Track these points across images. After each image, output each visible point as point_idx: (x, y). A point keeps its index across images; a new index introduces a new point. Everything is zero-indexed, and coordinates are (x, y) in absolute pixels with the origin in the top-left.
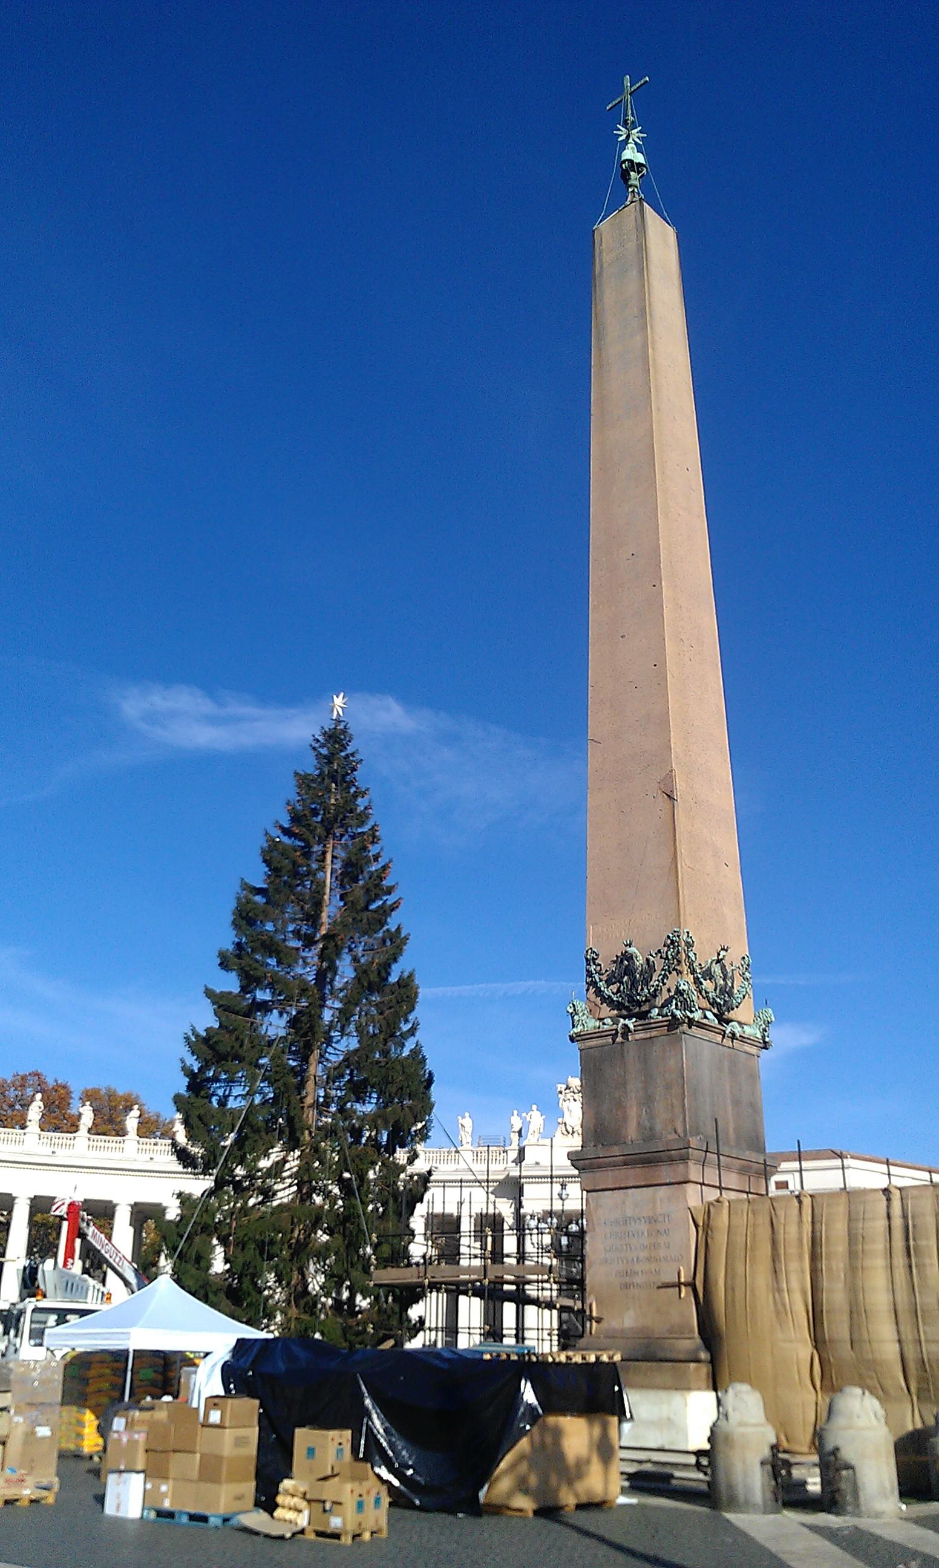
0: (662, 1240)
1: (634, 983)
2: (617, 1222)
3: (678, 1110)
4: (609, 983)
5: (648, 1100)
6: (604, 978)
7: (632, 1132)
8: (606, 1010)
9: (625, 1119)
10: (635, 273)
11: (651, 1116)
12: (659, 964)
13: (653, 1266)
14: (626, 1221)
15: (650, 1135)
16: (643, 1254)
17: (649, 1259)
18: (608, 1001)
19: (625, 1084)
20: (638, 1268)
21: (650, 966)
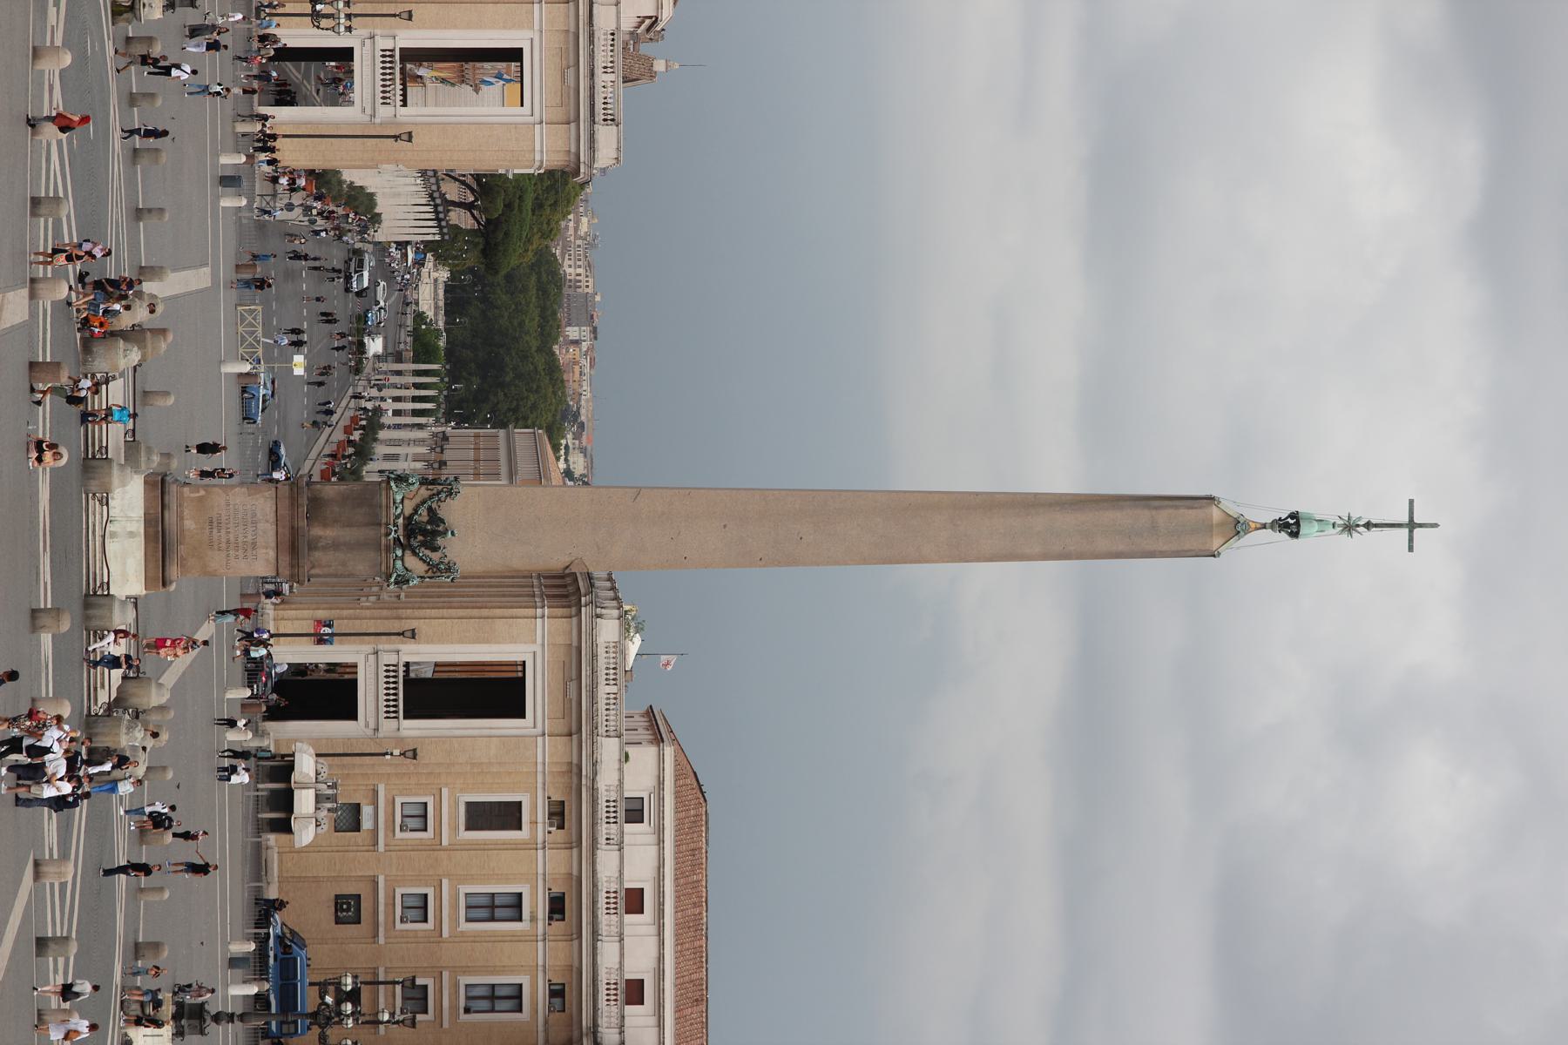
0: (240, 552)
1: (424, 532)
2: (254, 515)
3: (326, 570)
4: (430, 509)
5: (336, 546)
6: (434, 506)
7: (317, 531)
8: (408, 512)
9: (325, 526)
10: (1121, 548)
11: (325, 548)
12: (435, 556)
13: (223, 545)
14: (255, 523)
15: (312, 546)
16: (232, 537)
17: (228, 542)
18: (416, 511)
19: (350, 525)
20: (223, 532)
21: (435, 549)
